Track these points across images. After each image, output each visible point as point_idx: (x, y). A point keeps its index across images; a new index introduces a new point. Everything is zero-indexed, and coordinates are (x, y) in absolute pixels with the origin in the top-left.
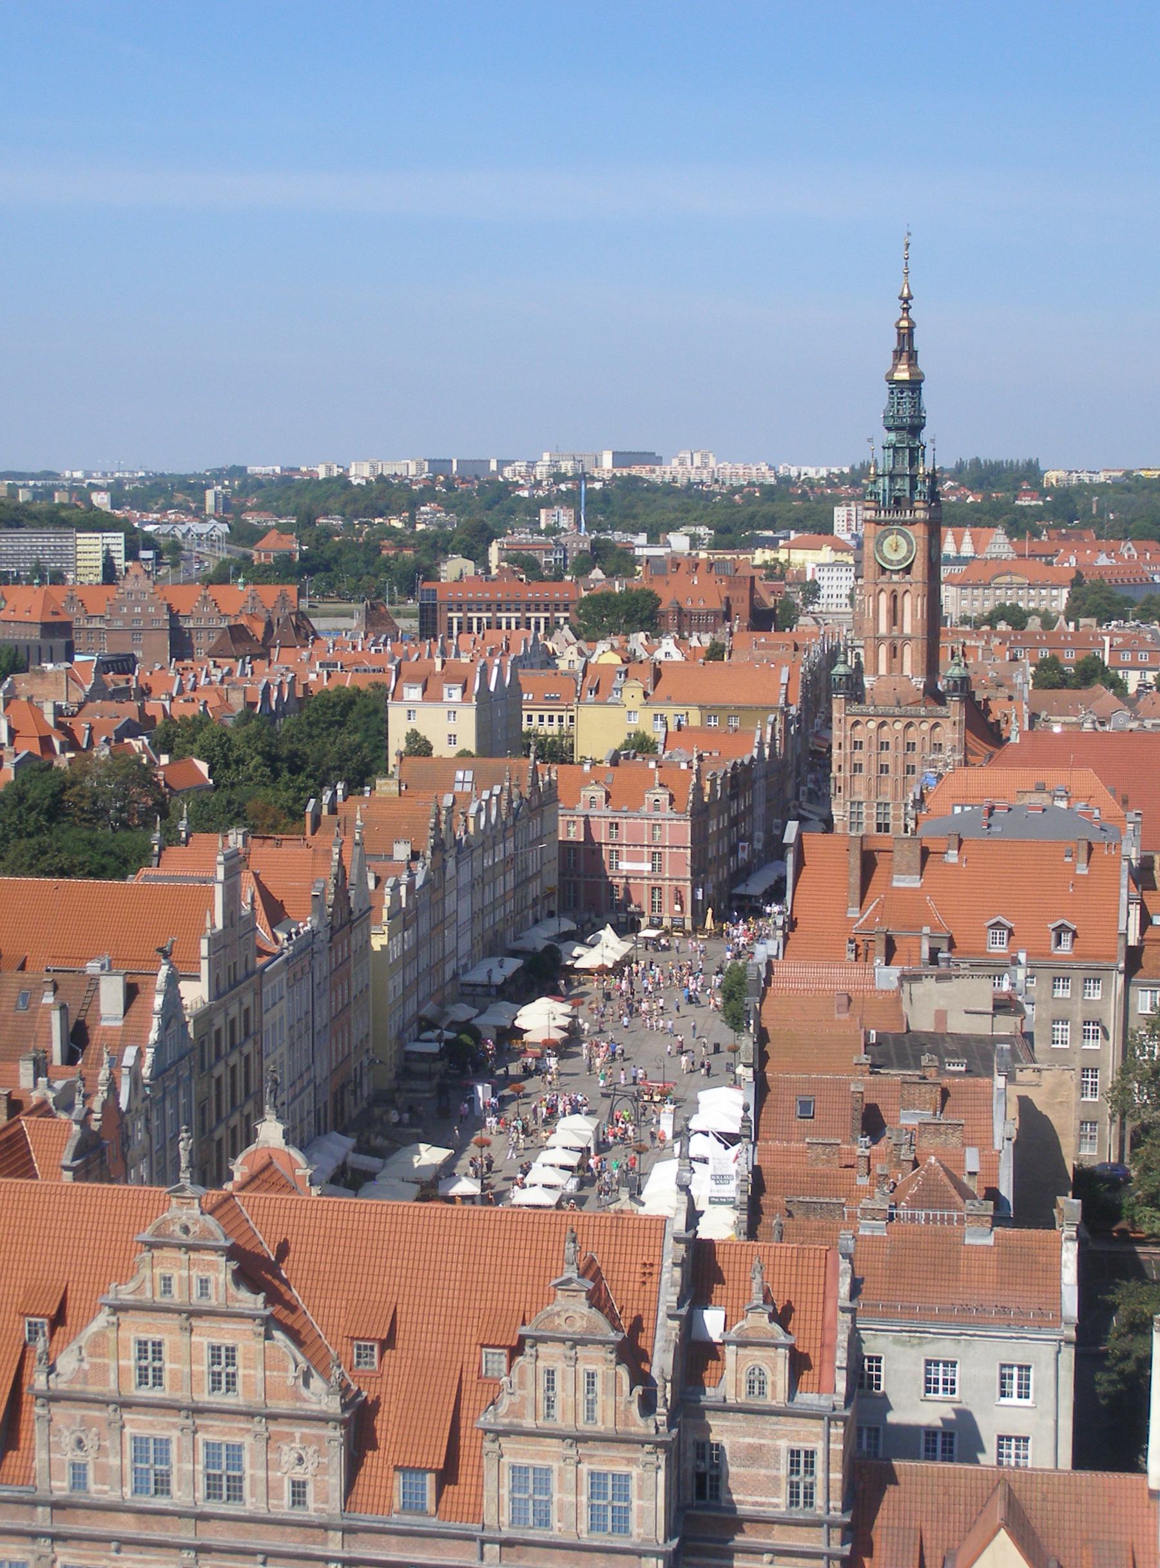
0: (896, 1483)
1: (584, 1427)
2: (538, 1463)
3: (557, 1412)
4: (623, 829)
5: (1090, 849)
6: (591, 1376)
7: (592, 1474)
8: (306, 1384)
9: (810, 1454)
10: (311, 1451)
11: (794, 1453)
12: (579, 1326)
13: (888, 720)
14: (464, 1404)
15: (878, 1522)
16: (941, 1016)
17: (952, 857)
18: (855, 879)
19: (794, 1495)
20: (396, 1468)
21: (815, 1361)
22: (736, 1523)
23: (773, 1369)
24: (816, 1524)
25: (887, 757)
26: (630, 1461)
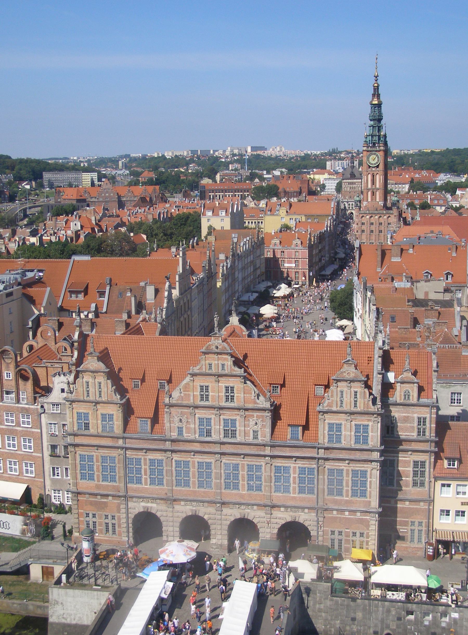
0: (450, 429)
1: (353, 409)
2: (337, 422)
3: (344, 405)
4: (286, 253)
5: (457, 248)
6: (356, 392)
7: (356, 425)
8: (258, 398)
9: (425, 419)
10: (260, 420)
11: (419, 418)
12: (352, 376)
13: (373, 215)
14: (310, 404)
15: (445, 441)
16: (426, 294)
17: (411, 251)
18: (379, 259)
19: (419, 432)
20: (289, 425)
21: (426, 388)
22: (400, 442)
23: (413, 391)
24: (427, 441)
25: (373, 228)
26: (369, 420)
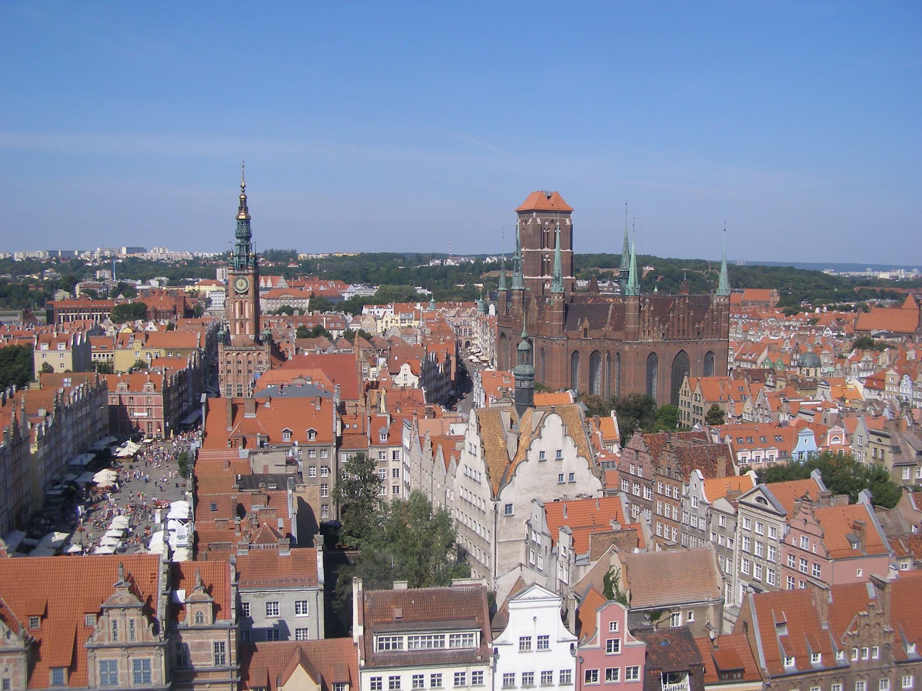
1: (129, 642)
2: (111, 658)
3: (118, 637)
4: (135, 400)
5: (321, 400)
6: (132, 621)
7: (134, 661)
8: (8, 637)
9: (223, 644)
10: (11, 665)
11: (216, 644)
12: (126, 601)
14: (79, 638)
15: (251, 667)
16: (266, 468)
17: (268, 405)
18: (230, 415)
19: (217, 660)
20: (50, 668)
21: (223, 607)
22: (194, 673)
23: (206, 612)
24: (227, 670)
25: (240, 367)
26: (150, 654)
